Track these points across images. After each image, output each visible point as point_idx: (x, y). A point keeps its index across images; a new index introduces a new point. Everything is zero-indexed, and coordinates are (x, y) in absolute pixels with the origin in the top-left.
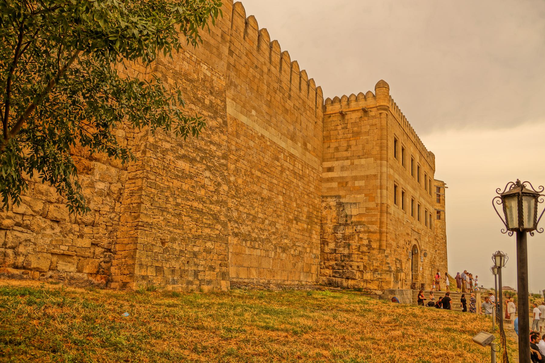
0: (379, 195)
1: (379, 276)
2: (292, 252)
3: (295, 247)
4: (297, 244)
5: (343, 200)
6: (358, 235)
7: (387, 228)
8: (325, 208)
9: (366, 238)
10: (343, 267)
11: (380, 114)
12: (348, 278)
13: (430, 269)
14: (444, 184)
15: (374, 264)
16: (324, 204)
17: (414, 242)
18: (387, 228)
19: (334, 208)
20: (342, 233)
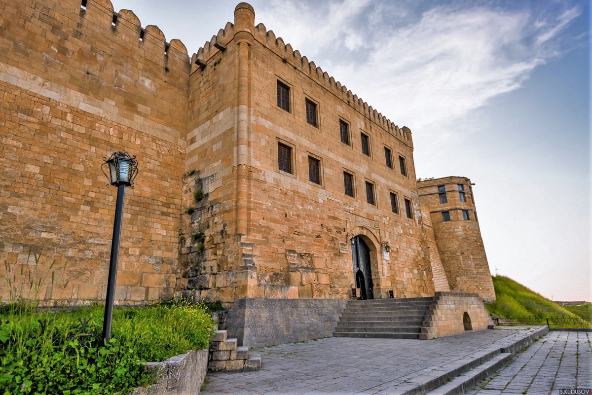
0: (235, 155)
1: (233, 279)
2: (70, 253)
3: (81, 246)
4: (90, 241)
5: (202, 176)
6: (213, 221)
7: (249, 202)
8: (186, 192)
9: (220, 221)
10: (197, 271)
11: (239, 44)
12: (201, 289)
13: (416, 271)
14: (467, 180)
15: (229, 260)
16: (185, 188)
17: (357, 232)
18: (249, 202)
19: (193, 190)
20: (198, 222)
